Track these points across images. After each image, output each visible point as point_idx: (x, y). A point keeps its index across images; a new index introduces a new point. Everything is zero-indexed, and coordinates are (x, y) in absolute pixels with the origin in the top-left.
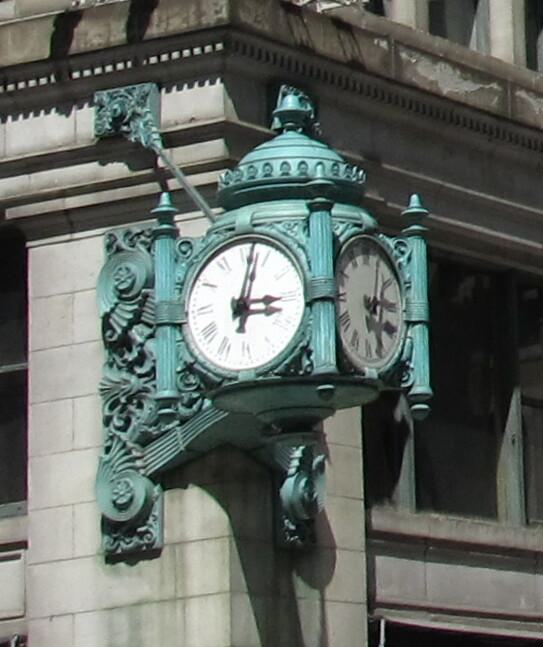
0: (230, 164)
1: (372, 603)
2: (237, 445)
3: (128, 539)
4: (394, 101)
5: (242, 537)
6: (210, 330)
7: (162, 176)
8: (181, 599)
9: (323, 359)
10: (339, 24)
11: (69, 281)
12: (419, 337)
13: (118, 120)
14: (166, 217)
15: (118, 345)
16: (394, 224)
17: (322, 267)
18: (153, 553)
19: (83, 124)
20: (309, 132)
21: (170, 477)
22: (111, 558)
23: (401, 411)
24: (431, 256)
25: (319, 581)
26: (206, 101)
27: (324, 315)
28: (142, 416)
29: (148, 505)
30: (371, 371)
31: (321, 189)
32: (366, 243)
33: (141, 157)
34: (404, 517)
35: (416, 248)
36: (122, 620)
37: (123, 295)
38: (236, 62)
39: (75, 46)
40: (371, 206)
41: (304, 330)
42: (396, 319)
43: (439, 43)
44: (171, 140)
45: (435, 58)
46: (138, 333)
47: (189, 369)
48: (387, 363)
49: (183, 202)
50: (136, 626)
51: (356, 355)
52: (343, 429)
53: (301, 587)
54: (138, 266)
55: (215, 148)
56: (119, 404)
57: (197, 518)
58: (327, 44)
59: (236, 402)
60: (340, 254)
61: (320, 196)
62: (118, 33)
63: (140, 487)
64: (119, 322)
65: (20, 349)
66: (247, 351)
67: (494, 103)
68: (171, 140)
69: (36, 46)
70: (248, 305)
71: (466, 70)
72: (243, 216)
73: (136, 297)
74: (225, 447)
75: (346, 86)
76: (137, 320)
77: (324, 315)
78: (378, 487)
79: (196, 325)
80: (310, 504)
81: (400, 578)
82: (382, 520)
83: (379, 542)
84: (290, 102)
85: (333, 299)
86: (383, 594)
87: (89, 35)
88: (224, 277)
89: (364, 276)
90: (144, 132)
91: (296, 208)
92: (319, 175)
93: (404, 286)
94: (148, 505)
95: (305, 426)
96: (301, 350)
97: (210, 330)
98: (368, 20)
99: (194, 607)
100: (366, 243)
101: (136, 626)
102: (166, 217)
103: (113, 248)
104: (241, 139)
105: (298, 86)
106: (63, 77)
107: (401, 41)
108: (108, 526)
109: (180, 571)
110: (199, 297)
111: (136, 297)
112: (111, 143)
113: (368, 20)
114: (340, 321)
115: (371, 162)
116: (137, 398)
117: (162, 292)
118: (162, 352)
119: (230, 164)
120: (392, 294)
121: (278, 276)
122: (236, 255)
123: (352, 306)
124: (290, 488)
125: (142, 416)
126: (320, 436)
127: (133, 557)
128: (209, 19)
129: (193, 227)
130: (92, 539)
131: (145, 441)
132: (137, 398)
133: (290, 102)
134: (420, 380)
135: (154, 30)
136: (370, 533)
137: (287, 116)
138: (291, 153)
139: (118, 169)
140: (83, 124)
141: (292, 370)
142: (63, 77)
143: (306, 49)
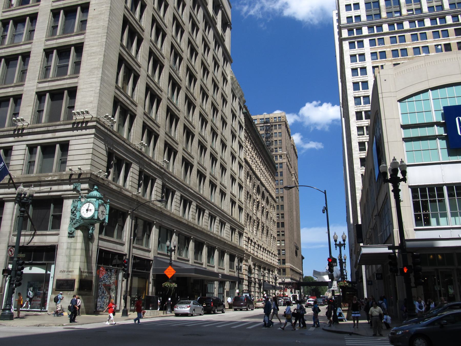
0: (88, 193)
1: (98, 246)
2: (85, 226)
3: (71, 235)
4: (107, 188)
5: (84, 236)
6: (83, 212)
7: (80, 194)
8: (76, 243)
9: (96, 217)
10: (102, 179)
11: (68, 205)
12: (107, 216)
13: (76, 187)
14: (80, 199)
15: (73, 213)
16: (106, 203)
17: (97, 207)
18: (74, 237)
19: (72, 187)
20: (97, 191)
21: (77, 229)
22: (69, 237)
23: (104, 224)
24: (110, 207)
25: (92, 243)
26: (86, 186)
27: (97, 212)
28: (74, 221)
29: (74, 231)
30: (101, 219)
31: (98, 198)
32: (102, 204)
33: (78, 191)
34: (103, 236)
35: (108, 206)
36: (69, 244)
37: (74, 207)
38: (90, 182)
39: (72, 178)
40: (103, 200)
41: (94, 214)
42: (105, 214)
43: (113, 183)
44: (82, 190)
45: (113, 184)
46: (75, 212)
47: (80, 216)
48: (103, 218)
49: (82, 197)
50: (71, 245)
51: (100, 217)
52: (97, 225)
53: (90, 243)
54: (76, 204)
55: (86, 191)
56: (72, 219)
57: (79, 233)
58: (101, 181)
59: (85, 221)
60: (99, 205)
61: (98, 198)
62: (77, 177)
63: (73, 229)
64: (73, 210)
65: (61, 211)
66: (87, 215)
67: (119, 190)
68: (82, 190)
69: (68, 177)
70: (88, 210)
71: (116, 186)
72: (89, 200)
73: (75, 207)
74: (83, 226)
75: (102, 186)
76: (75, 210)
77: (97, 212)
78: (100, 233)
79: (82, 211)
80: (92, 234)
81: (102, 243)
82: (100, 236)
83: (100, 239)
84: (96, 187)
85: (98, 210)
86: (99, 245)
87: (74, 177)
88: (86, 206)
89: (102, 208)
90: (79, 189)
91: (95, 199)
92: (98, 196)
93: (106, 210)
94: (74, 231)
95: (93, 225)
96: (93, 216)
97: (83, 212)
98: (106, 179)
99: (78, 244)
100: (102, 204)
101: (71, 245)
102: (80, 199)
103: (73, 201)
104: (89, 191)
105: (97, 186)
106: (70, 181)
107: (109, 182)
108: (69, 233)
109: (77, 239)
110: (82, 208)
111: (75, 207)
112: (75, 189)
113: (106, 179)
114: (98, 213)
115: (104, 195)
116: (74, 219)
117: (78, 207)
118: (78, 214)
119: (88, 193)
120: (105, 211)
121: (92, 207)
122: (87, 204)
123: (100, 211)
124: (90, 231)
125: (74, 221)
126: (94, 226)
127: (71, 237)
128: (88, 177)
129: (83, 200)
130: (67, 234)
131: (74, 224)
132: (74, 219)
133: (96, 187)
134: (107, 221)
135: (81, 177)
136: (99, 238)
137: (95, 189)
138: (95, 193)
139: (75, 193)
140: (72, 187)
141: (92, 218)
142: (70, 181)
143: (98, 181)
